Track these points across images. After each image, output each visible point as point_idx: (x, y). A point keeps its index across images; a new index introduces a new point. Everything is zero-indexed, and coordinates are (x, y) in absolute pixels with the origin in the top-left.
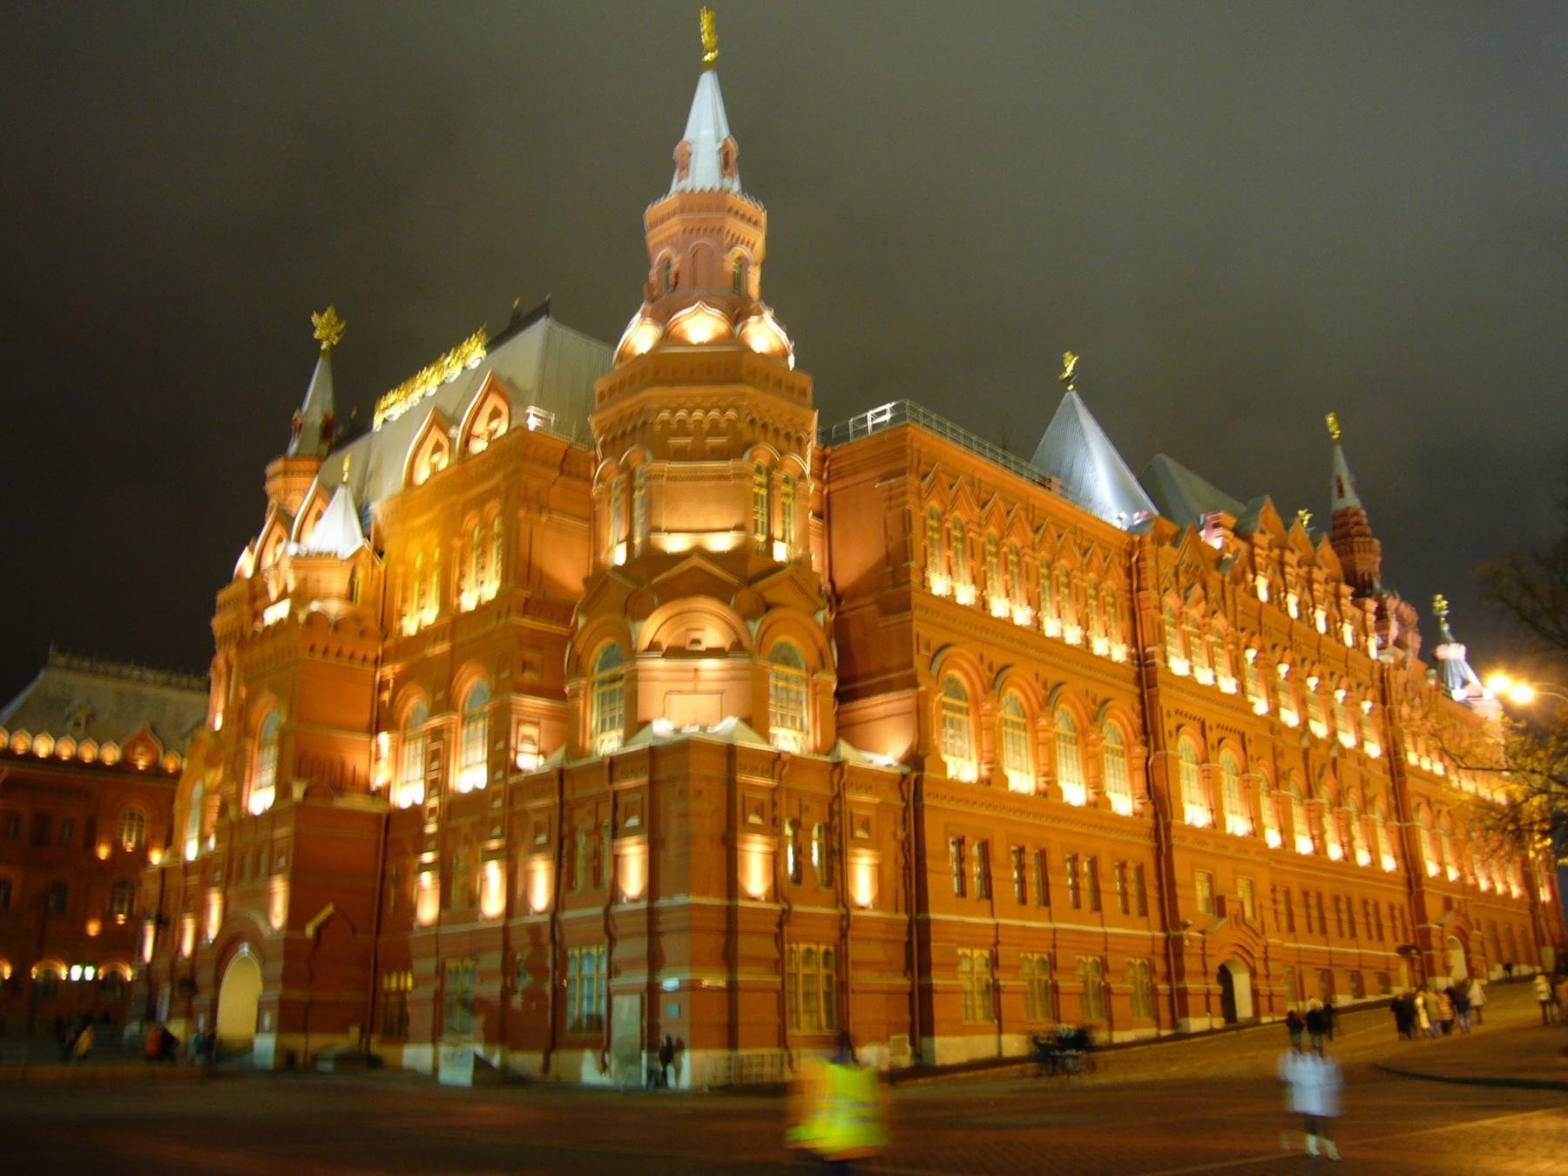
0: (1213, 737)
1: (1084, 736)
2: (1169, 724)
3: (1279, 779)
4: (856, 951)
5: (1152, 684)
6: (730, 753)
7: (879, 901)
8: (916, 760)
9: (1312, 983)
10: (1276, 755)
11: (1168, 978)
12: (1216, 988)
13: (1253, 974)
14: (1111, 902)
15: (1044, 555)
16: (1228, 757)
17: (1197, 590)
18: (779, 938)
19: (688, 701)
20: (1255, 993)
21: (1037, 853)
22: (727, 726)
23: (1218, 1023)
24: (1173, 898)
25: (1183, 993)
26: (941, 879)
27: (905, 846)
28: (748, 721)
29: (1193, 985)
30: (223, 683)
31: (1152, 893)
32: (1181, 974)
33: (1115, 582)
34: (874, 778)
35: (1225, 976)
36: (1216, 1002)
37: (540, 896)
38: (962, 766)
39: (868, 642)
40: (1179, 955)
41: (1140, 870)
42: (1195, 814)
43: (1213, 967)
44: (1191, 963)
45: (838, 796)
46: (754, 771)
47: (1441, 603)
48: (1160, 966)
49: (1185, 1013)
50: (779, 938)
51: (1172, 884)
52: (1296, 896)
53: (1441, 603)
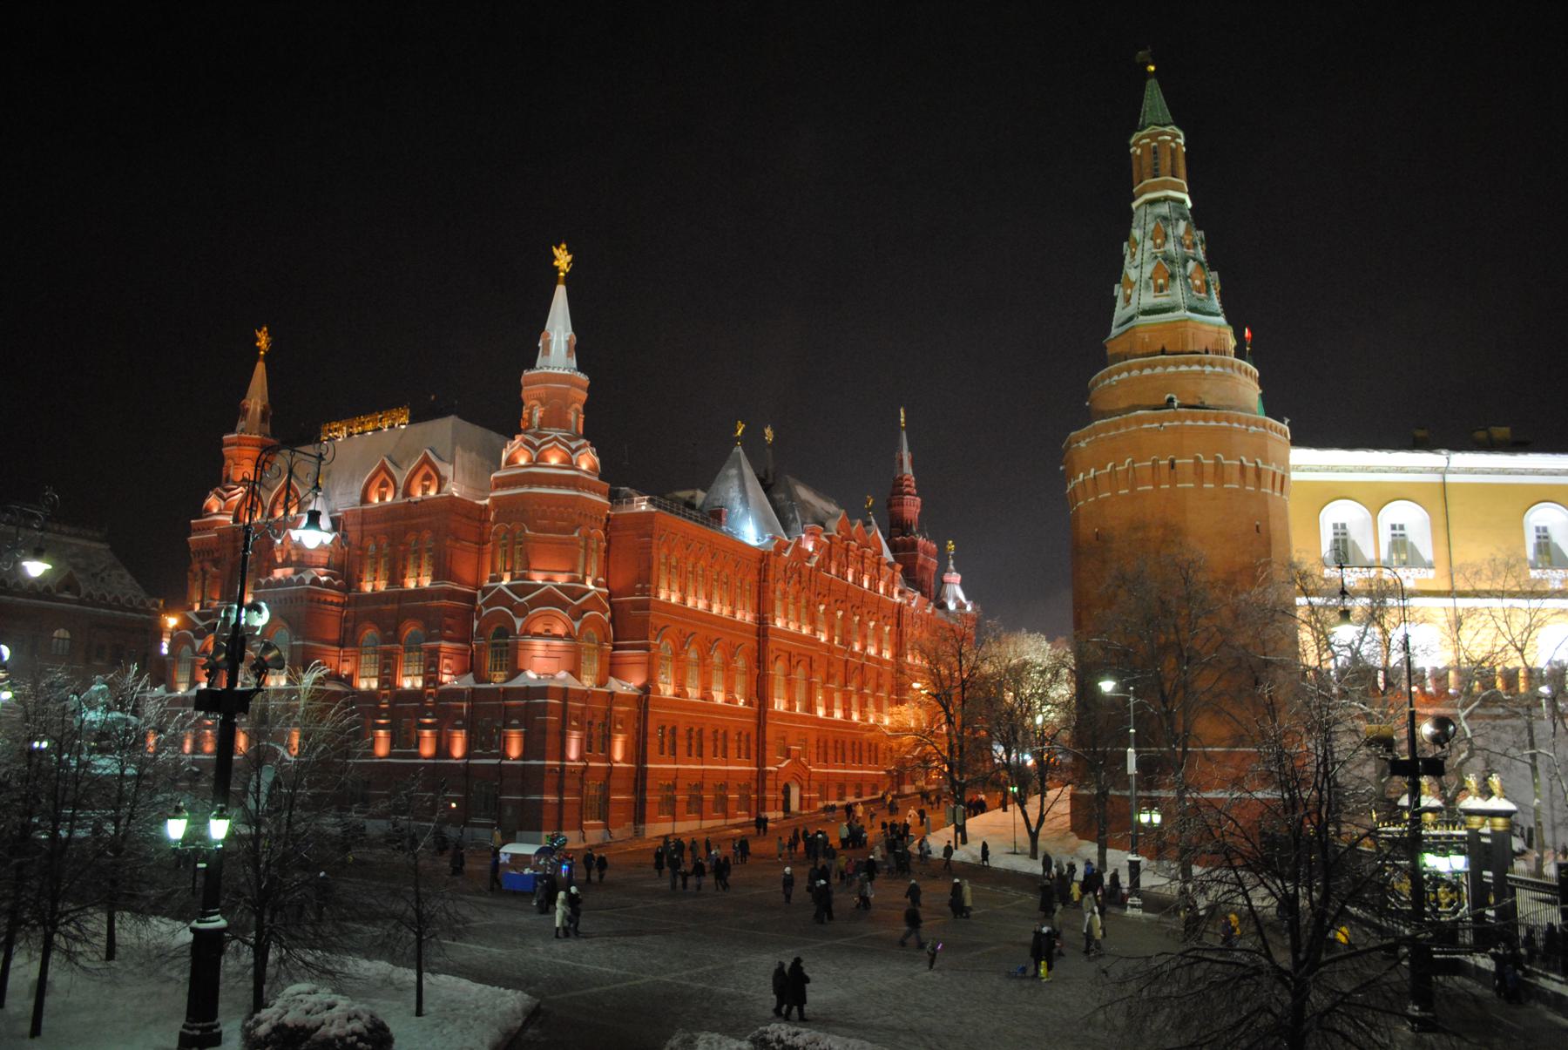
0: (794, 662)
1: (727, 666)
2: (772, 657)
3: (829, 677)
4: (614, 783)
5: (765, 635)
6: (565, 693)
7: (624, 760)
8: (646, 689)
9: (833, 791)
10: (830, 664)
11: (757, 791)
12: (781, 797)
13: (802, 788)
14: (732, 753)
15: (717, 568)
16: (800, 674)
17: (795, 576)
18: (581, 779)
19: (542, 664)
20: (801, 798)
21: (699, 733)
22: (562, 677)
23: (781, 814)
24: (764, 749)
25: (764, 799)
26: (653, 748)
27: (638, 733)
28: (571, 672)
29: (770, 796)
30: (198, 584)
31: (753, 746)
32: (764, 788)
33: (751, 578)
34: (624, 699)
35: (786, 791)
36: (780, 805)
37: (458, 750)
38: (667, 690)
39: (627, 624)
40: (764, 781)
41: (748, 735)
42: (780, 705)
43: (781, 785)
44: (769, 784)
45: (610, 710)
46: (575, 700)
47: (951, 546)
48: (754, 785)
49: (764, 810)
50: (581, 779)
51: (764, 742)
52: (831, 743)
53: (951, 546)
